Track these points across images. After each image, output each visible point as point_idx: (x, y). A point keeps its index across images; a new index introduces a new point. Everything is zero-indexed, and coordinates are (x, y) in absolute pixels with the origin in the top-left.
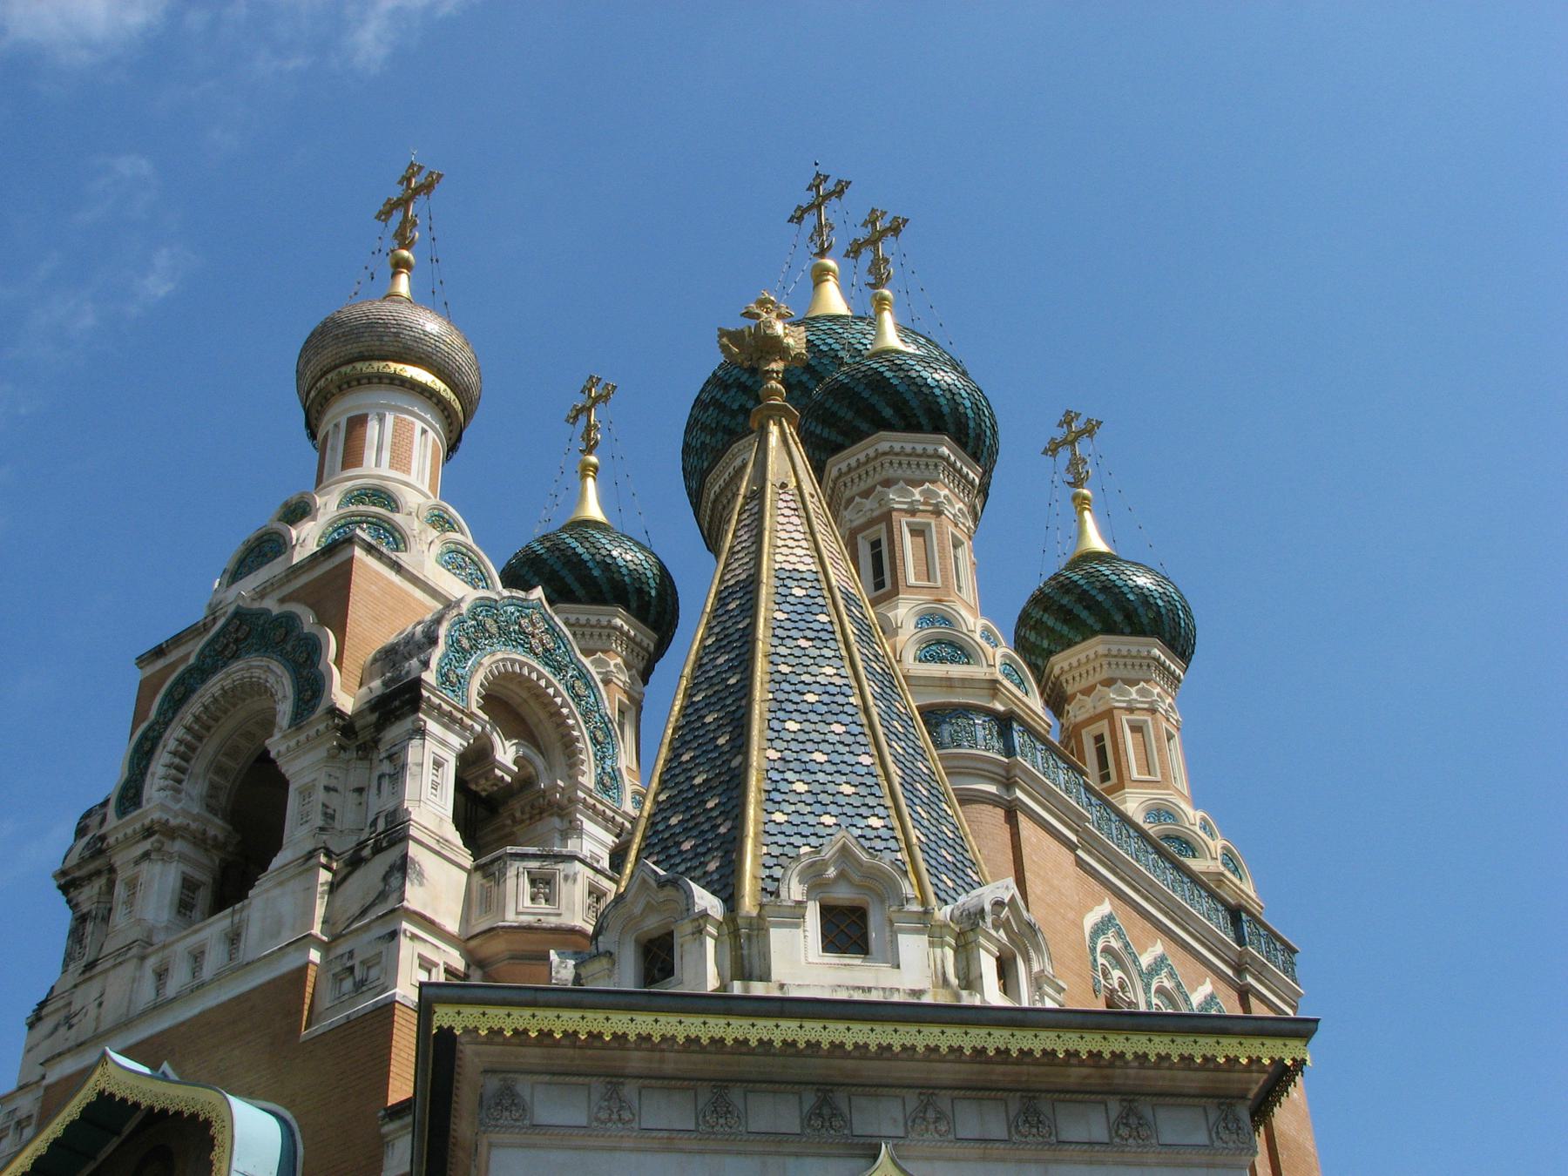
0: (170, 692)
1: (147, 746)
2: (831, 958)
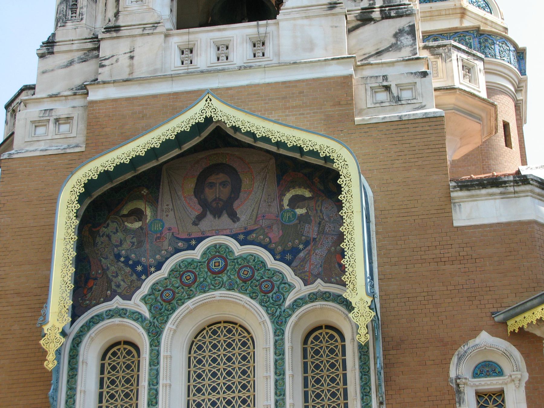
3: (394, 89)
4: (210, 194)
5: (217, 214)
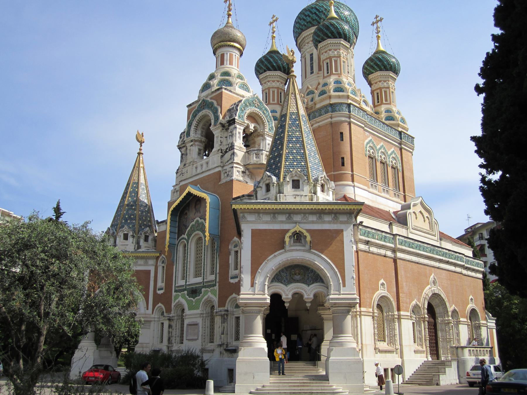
0: (193, 114)
1: (190, 124)
2: (293, 190)
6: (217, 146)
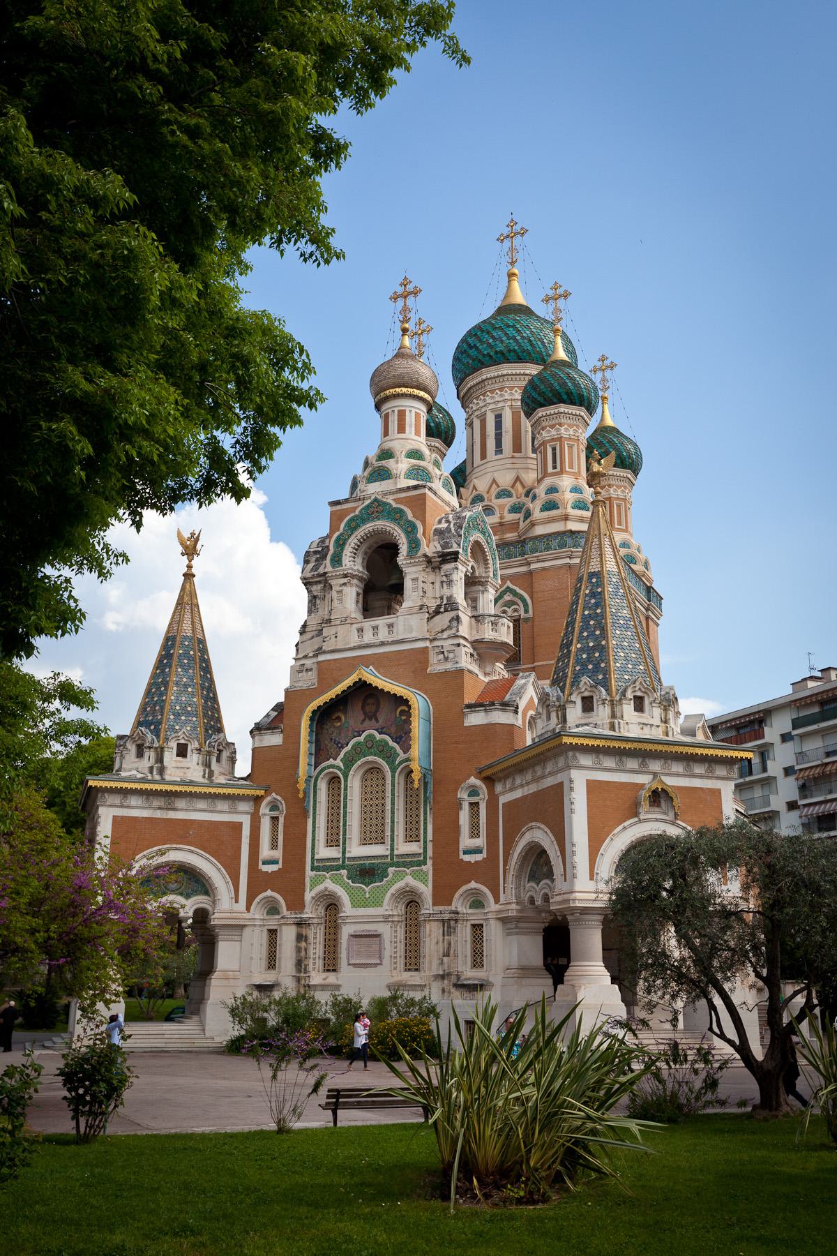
0: (348, 521)
1: (341, 542)
2: (636, 713)
3: (446, 653)
4: (368, 709)
5: (370, 719)
6: (411, 597)
